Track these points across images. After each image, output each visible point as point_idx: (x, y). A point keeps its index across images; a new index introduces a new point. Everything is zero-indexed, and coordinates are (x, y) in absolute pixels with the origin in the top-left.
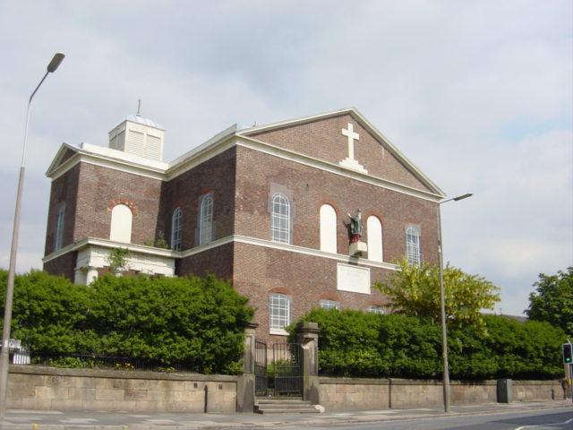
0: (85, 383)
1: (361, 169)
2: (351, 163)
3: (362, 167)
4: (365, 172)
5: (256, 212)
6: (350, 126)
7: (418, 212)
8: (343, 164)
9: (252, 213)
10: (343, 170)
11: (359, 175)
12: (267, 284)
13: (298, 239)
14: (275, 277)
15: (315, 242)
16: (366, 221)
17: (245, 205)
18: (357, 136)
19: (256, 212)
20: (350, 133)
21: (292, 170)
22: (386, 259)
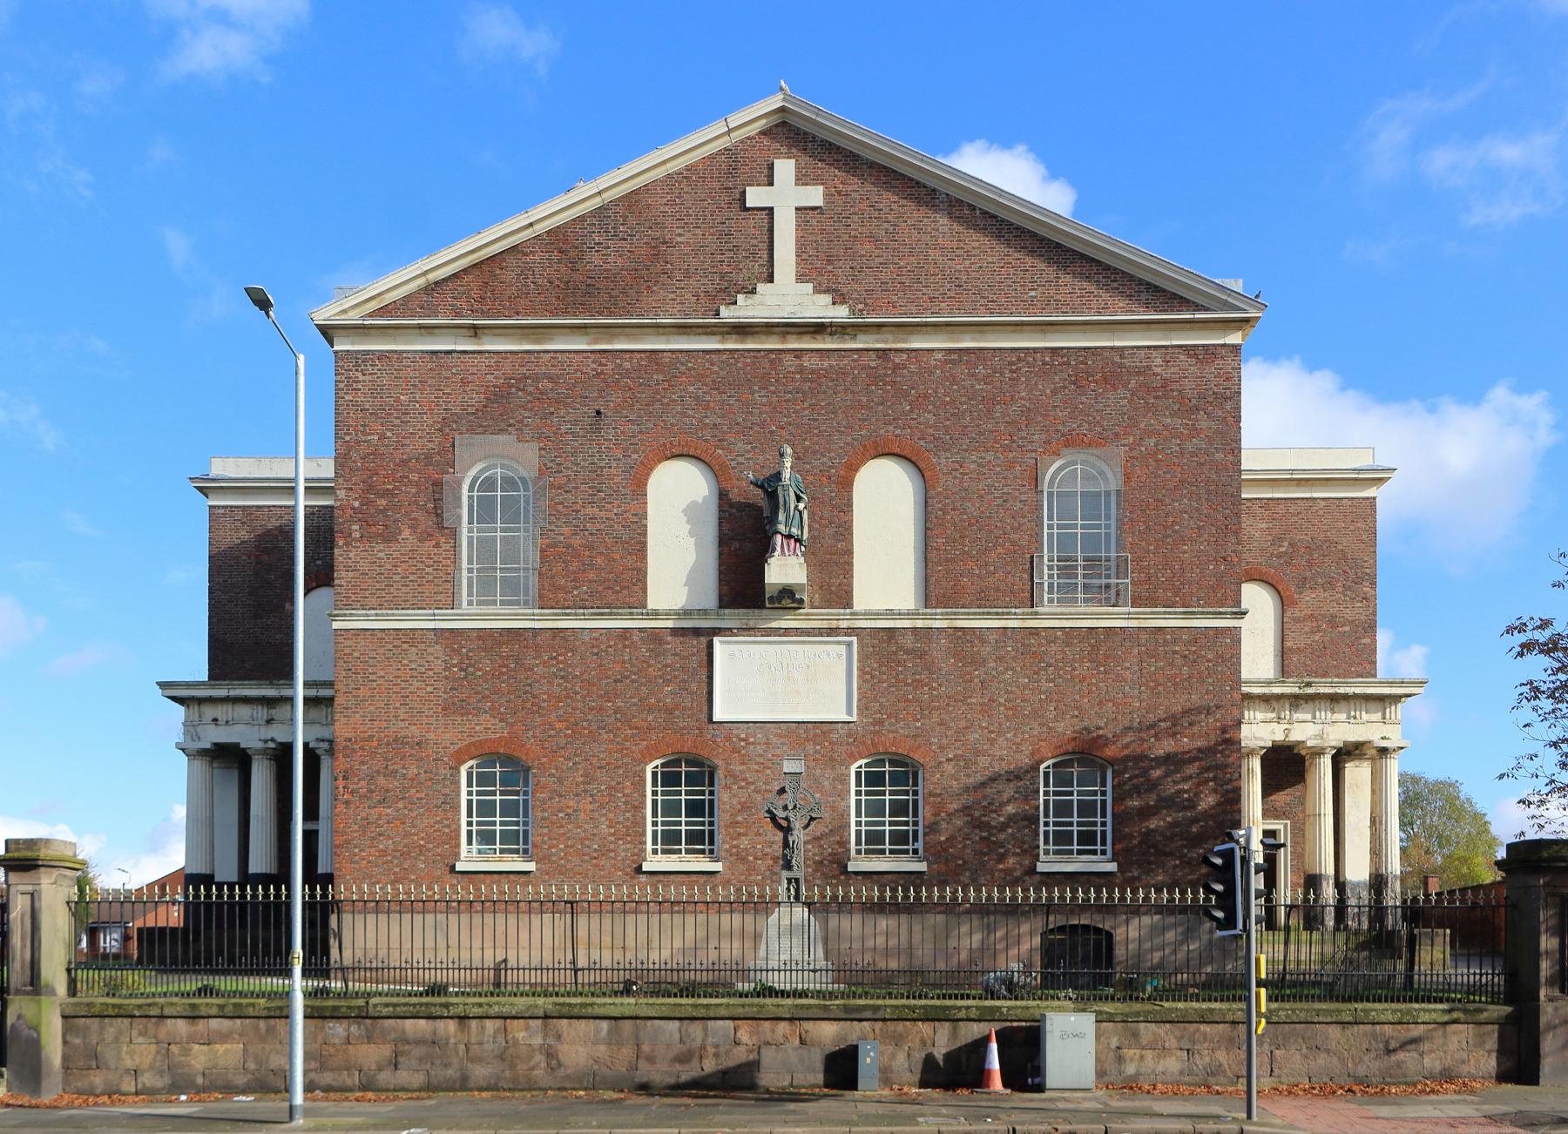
0: (1553, 952)
1: (820, 308)
2: (787, 296)
3: (827, 299)
4: (841, 313)
5: (406, 533)
6: (785, 168)
7: (1118, 399)
8: (745, 309)
9: (389, 537)
10: (742, 330)
11: (818, 329)
12: (447, 734)
13: (557, 588)
14: (479, 711)
15: (627, 584)
16: (847, 484)
17: (366, 522)
18: (814, 196)
19: (406, 533)
20: (787, 193)
21: (536, 379)
22: (934, 591)
